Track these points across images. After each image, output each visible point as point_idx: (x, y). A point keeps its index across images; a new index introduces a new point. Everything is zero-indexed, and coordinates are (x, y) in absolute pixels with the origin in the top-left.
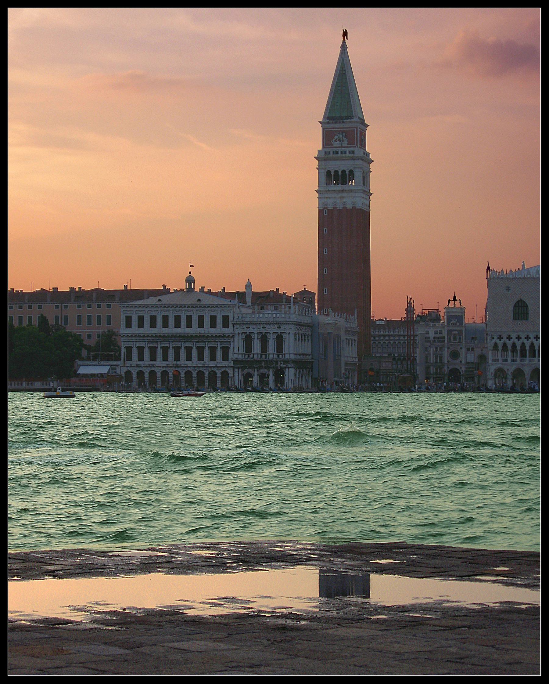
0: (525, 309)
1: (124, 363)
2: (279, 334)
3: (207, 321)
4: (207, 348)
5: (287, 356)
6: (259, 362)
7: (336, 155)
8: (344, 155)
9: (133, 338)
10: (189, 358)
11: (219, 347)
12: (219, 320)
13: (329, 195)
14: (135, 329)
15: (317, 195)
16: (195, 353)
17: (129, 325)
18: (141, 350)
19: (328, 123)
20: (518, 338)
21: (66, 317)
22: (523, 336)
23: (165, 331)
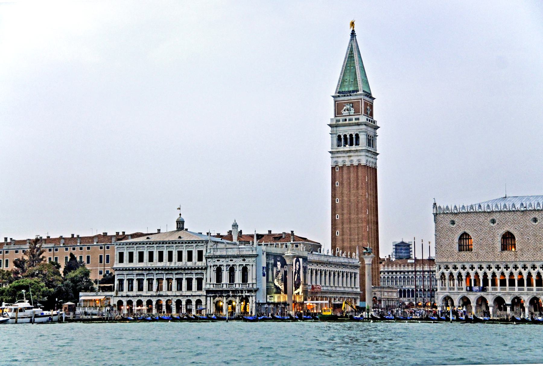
1: (117, 294)
2: (244, 265)
3: (185, 255)
4: (184, 279)
5: (251, 286)
6: (228, 291)
7: (345, 122)
8: (351, 122)
9: (124, 272)
10: (170, 289)
11: (194, 278)
12: (195, 255)
14: (126, 264)
15: (330, 155)
17: (121, 260)
18: (130, 281)
19: (339, 96)
21: (108, 256)
23: (149, 265)
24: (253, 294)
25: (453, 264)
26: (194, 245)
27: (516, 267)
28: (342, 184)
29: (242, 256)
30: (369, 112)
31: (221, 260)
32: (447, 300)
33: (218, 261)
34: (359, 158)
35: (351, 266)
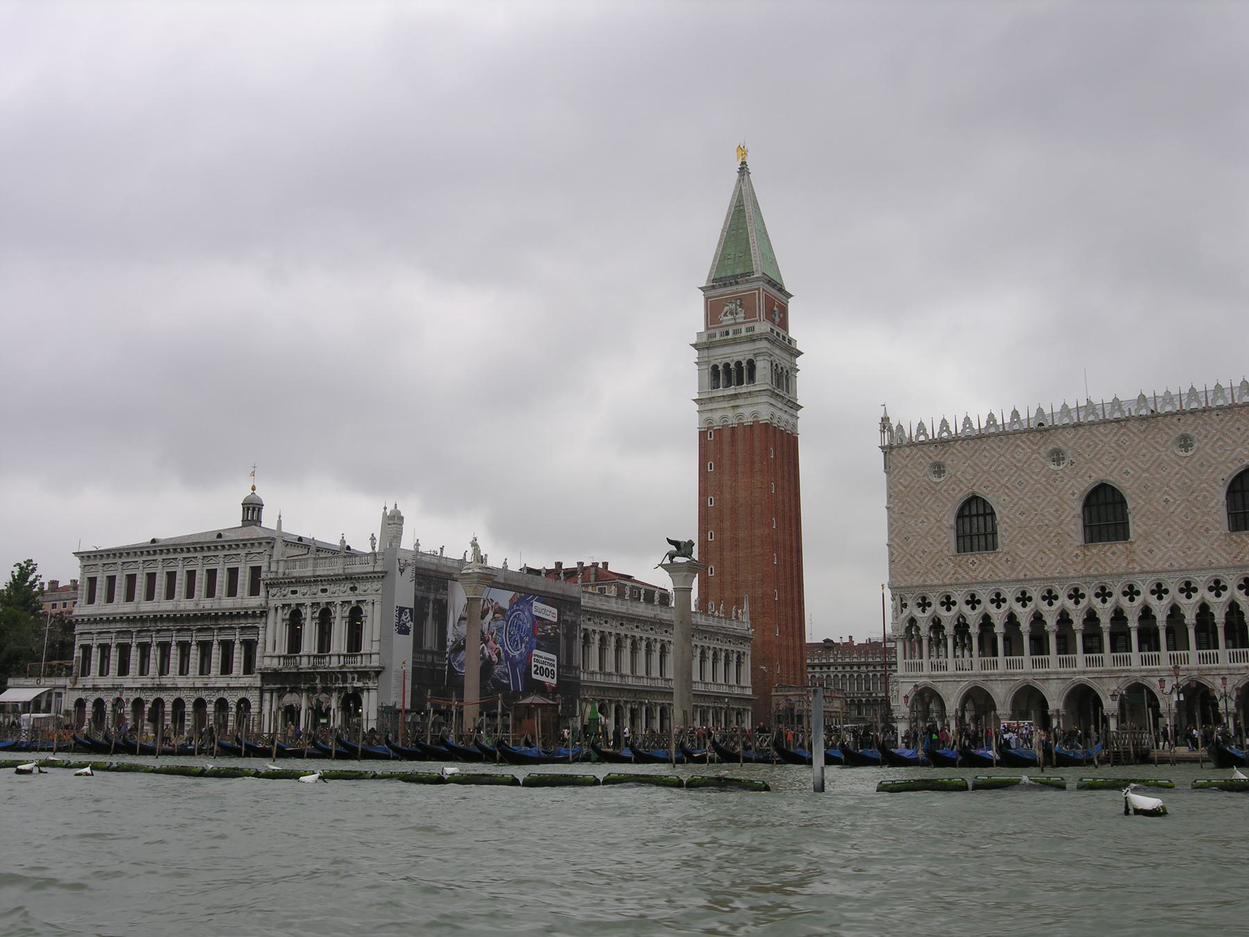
0: (989, 524)
3: (222, 579)
4: (215, 646)
6: (309, 676)
9: (93, 627)
10: (183, 671)
12: (244, 579)
13: (715, 406)
14: (100, 608)
15: (696, 407)
16: (195, 655)
20: (973, 602)
22: (985, 596)
24: (370, 685)
25: (942, 590)
26: (243, 552)
27: (1131, 593)
28: (719, 465)
29: (348, 578)
30: (777, 320)
31: (302, 589)
32: (926, 698)
33: (294, 592)
34: (755, 409)
35: (725, 635)
